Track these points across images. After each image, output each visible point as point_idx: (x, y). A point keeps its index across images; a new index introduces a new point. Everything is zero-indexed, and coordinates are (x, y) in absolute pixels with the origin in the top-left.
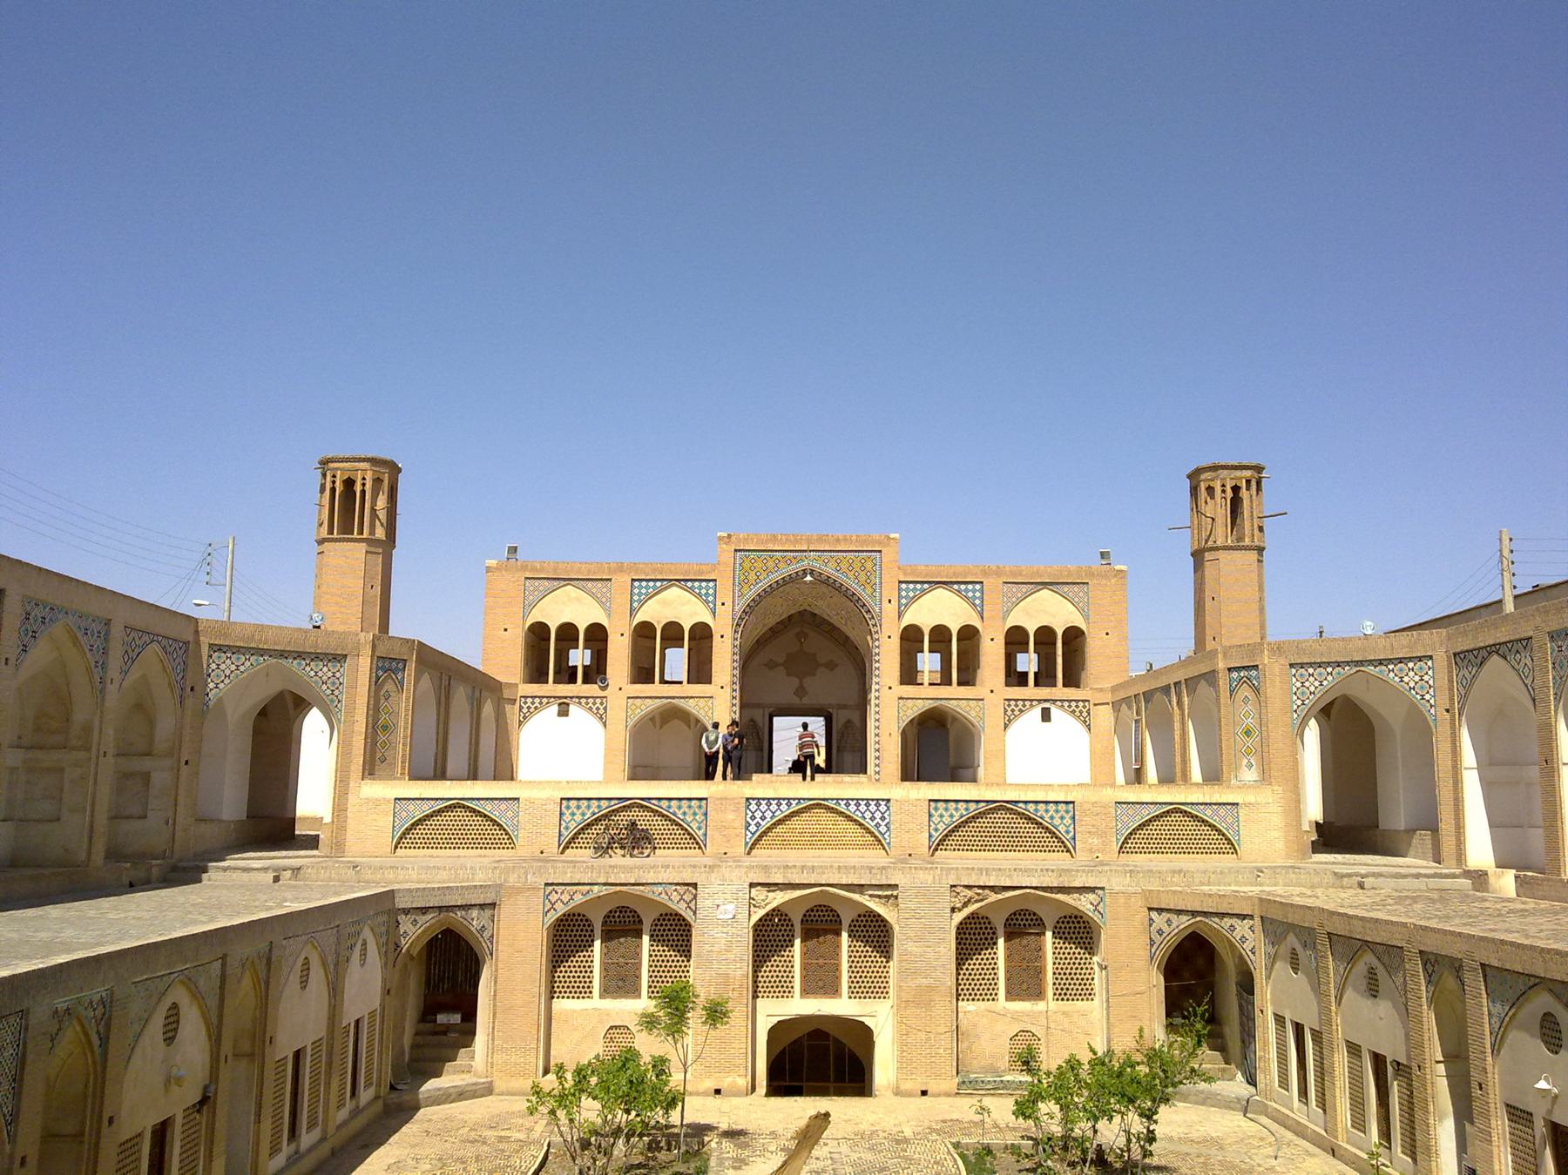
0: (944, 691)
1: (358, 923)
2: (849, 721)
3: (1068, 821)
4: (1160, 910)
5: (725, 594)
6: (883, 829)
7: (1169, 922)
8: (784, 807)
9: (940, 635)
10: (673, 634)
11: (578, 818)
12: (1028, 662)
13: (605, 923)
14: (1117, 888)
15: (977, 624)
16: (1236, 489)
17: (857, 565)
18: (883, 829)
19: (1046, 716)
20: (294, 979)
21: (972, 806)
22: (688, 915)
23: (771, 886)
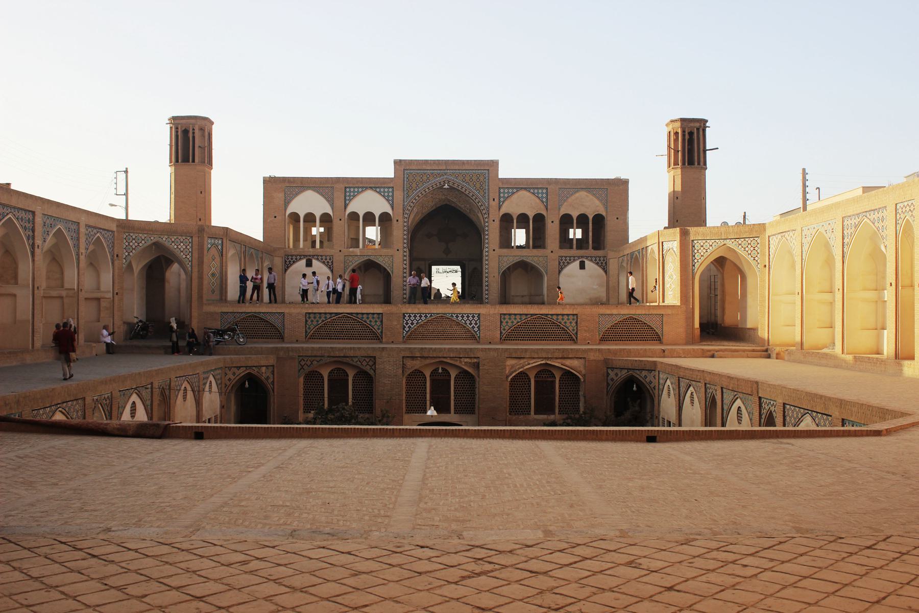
0: (525, 252)
1: (207, 372)
2: (475, 269)
3: (574, 324)
4: (612, 369)
5: (399, 195)
6: (476, 329)
7: (617, 375)
8: (423, 318)
9: (523, 220)
10: (369, 219)
11: (315, 323)
12: (576, 233)
13: (329, 376)
14: (592, 358)
15: (544, 213)
16: (691, 134)
17: (474, 178)
18: (476, 329)
19: (582, 266)
20: (180, 397)
21: (524, 317)
22: (371, 372)
23: (413, 358)
